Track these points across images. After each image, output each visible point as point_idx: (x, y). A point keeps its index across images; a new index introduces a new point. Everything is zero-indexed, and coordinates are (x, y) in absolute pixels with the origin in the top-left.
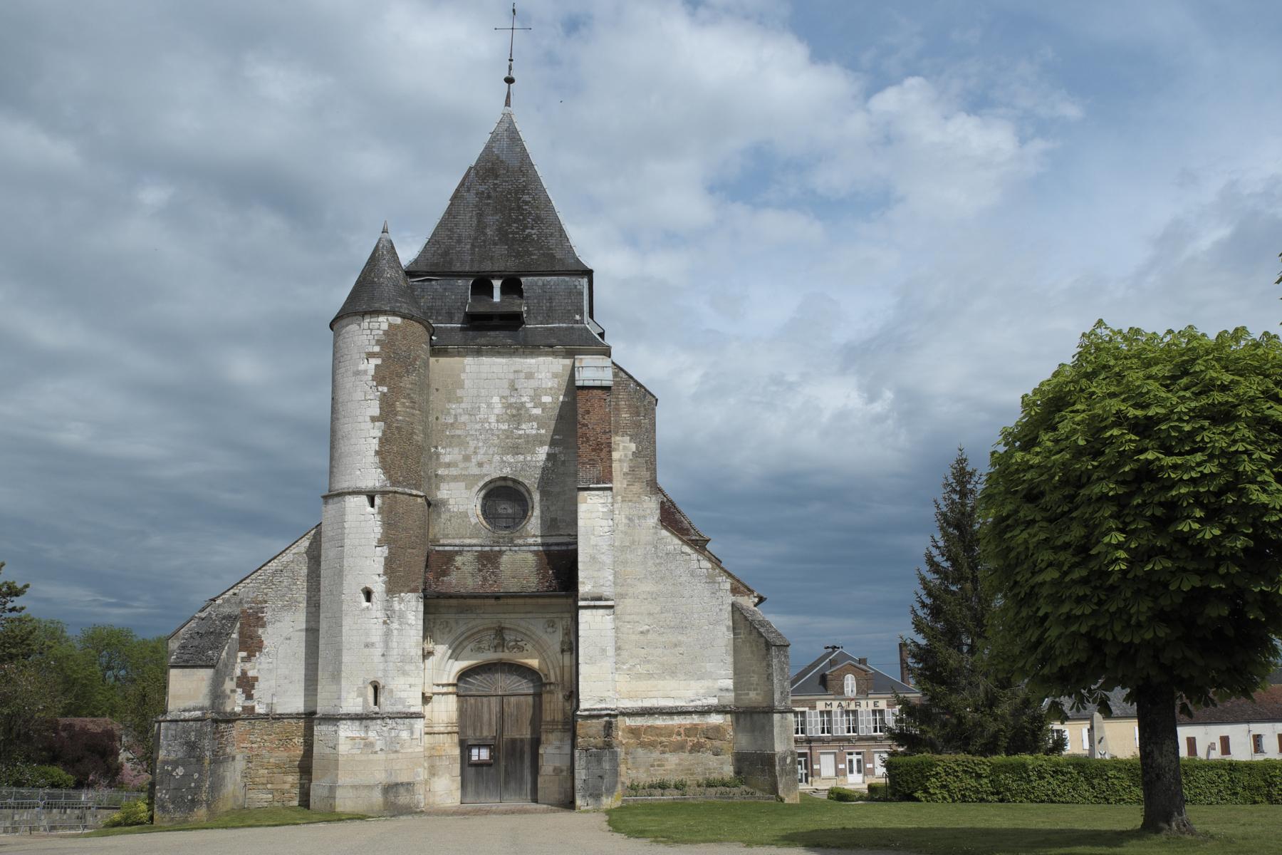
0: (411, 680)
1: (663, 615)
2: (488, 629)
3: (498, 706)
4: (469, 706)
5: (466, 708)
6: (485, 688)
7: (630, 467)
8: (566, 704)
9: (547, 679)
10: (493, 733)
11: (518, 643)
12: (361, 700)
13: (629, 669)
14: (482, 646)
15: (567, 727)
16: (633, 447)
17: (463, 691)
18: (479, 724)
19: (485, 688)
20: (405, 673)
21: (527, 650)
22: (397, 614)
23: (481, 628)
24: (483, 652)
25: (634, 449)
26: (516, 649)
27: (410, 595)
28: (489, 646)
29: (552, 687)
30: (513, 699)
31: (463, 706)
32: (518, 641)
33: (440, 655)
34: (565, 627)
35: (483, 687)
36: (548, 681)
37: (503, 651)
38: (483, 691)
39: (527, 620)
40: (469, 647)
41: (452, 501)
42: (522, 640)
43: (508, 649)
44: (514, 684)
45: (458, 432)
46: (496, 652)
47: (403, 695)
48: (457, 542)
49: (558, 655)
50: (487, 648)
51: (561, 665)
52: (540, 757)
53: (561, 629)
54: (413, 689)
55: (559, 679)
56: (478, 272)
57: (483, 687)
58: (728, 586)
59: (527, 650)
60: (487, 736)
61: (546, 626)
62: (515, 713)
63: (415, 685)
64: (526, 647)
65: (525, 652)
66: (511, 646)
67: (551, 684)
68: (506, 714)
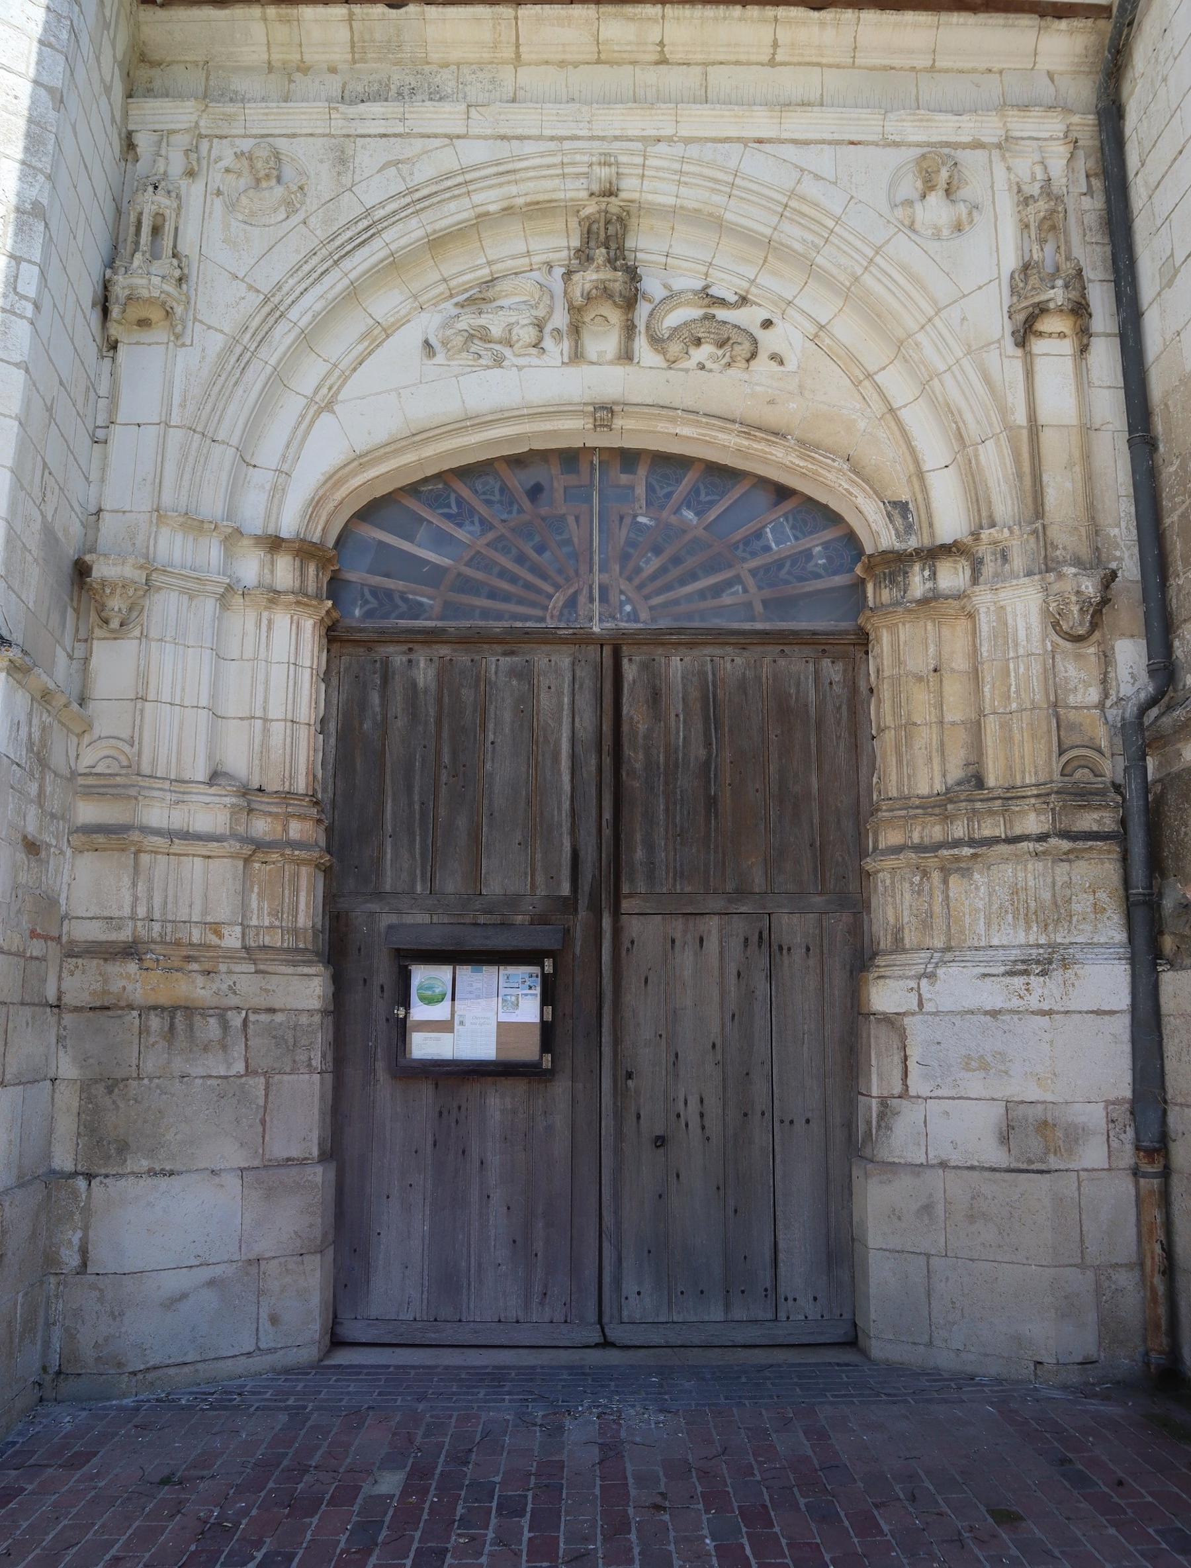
2: (537, 210)
3: (585, 701)
4: (398, 704)
5: (384, 725)
6: (507, 598)
8: (1070, 670)
9: (909, 528)
10: (552, 879)
11: (721, 314)
14: (496, 325)
15: (1088, 821)
17: (369, 614)
18: (462, 822)
19: (507, 598)
21: (777, 359)
23: (490, 199)
24: (499, 362)
26: (707, 349)
28: (540, 326)
29: (952, 576)
30: (676, 666)
31: (363, 705)
32: (722, 302)
33: (216, 342)
34: (1035, 190)
35: (493, 595)
36: (913, 543)
37: (627, 356)
38: (486, 614)
39: (789, 151)
40: (410, 337)
42: (744, 300)
43: (657, 342)
44: (693, 576)
46: (577, 356)
49: (992, 358)
50: (527, 334)
51: (1021, 418)
52: (879, 1042)
53: (1006, 205)
55: (1004, 504)
57: (493, 595)
59: (777, 359)
60: (513, 901)
61: (910, 186)
62: (698, 752)
64: (769, 341)
65: (762, 364)
66: (675, 330)
67: (934, 554)
68: (635, 758)
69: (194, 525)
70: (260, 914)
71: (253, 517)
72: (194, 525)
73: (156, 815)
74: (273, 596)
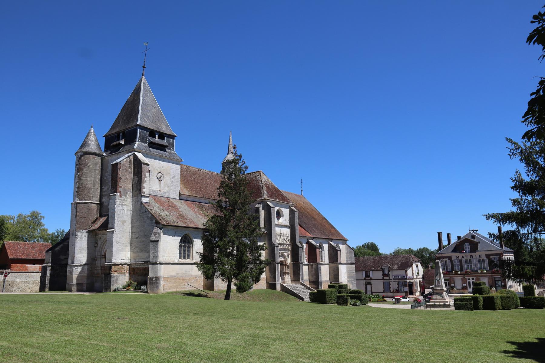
0: (83, 255)
1: (141, 232)
7: (136, 186)
12: (71, 260)
13: (133, 250)
16: (137, 179)
20: (81, 253)
22: (79, 236)
25: (137, 180)
27: (84, 231)
41: (105, 202)
45: (107, 182)
47: (81, 259)
48: (105, 214)
54: (84, 257)
56: (117, 132)
58: (154, 221)
63: (85, 256)
69: (99, 255)
70: (102, 272)
71: (102, 254)
72: (99, 255)
73: (98, 268)
74: (103, 258)
